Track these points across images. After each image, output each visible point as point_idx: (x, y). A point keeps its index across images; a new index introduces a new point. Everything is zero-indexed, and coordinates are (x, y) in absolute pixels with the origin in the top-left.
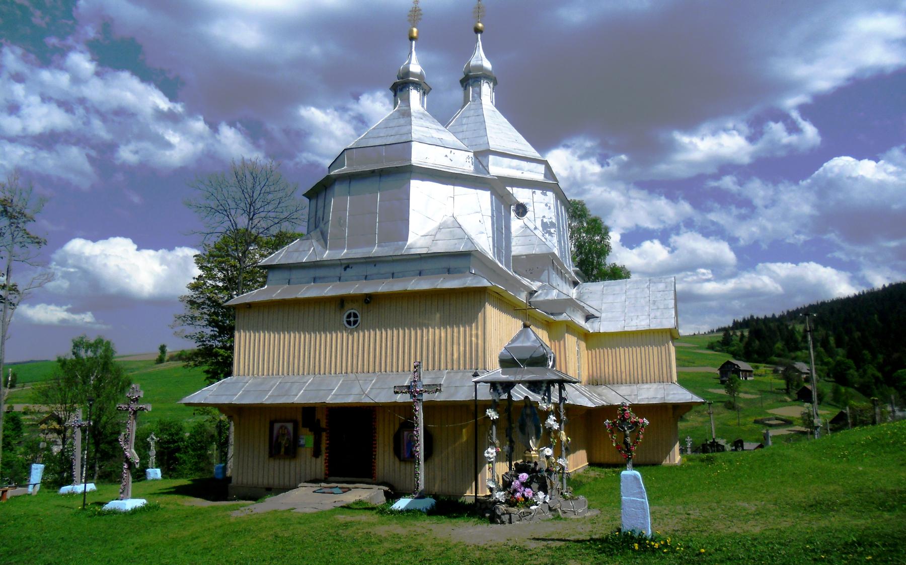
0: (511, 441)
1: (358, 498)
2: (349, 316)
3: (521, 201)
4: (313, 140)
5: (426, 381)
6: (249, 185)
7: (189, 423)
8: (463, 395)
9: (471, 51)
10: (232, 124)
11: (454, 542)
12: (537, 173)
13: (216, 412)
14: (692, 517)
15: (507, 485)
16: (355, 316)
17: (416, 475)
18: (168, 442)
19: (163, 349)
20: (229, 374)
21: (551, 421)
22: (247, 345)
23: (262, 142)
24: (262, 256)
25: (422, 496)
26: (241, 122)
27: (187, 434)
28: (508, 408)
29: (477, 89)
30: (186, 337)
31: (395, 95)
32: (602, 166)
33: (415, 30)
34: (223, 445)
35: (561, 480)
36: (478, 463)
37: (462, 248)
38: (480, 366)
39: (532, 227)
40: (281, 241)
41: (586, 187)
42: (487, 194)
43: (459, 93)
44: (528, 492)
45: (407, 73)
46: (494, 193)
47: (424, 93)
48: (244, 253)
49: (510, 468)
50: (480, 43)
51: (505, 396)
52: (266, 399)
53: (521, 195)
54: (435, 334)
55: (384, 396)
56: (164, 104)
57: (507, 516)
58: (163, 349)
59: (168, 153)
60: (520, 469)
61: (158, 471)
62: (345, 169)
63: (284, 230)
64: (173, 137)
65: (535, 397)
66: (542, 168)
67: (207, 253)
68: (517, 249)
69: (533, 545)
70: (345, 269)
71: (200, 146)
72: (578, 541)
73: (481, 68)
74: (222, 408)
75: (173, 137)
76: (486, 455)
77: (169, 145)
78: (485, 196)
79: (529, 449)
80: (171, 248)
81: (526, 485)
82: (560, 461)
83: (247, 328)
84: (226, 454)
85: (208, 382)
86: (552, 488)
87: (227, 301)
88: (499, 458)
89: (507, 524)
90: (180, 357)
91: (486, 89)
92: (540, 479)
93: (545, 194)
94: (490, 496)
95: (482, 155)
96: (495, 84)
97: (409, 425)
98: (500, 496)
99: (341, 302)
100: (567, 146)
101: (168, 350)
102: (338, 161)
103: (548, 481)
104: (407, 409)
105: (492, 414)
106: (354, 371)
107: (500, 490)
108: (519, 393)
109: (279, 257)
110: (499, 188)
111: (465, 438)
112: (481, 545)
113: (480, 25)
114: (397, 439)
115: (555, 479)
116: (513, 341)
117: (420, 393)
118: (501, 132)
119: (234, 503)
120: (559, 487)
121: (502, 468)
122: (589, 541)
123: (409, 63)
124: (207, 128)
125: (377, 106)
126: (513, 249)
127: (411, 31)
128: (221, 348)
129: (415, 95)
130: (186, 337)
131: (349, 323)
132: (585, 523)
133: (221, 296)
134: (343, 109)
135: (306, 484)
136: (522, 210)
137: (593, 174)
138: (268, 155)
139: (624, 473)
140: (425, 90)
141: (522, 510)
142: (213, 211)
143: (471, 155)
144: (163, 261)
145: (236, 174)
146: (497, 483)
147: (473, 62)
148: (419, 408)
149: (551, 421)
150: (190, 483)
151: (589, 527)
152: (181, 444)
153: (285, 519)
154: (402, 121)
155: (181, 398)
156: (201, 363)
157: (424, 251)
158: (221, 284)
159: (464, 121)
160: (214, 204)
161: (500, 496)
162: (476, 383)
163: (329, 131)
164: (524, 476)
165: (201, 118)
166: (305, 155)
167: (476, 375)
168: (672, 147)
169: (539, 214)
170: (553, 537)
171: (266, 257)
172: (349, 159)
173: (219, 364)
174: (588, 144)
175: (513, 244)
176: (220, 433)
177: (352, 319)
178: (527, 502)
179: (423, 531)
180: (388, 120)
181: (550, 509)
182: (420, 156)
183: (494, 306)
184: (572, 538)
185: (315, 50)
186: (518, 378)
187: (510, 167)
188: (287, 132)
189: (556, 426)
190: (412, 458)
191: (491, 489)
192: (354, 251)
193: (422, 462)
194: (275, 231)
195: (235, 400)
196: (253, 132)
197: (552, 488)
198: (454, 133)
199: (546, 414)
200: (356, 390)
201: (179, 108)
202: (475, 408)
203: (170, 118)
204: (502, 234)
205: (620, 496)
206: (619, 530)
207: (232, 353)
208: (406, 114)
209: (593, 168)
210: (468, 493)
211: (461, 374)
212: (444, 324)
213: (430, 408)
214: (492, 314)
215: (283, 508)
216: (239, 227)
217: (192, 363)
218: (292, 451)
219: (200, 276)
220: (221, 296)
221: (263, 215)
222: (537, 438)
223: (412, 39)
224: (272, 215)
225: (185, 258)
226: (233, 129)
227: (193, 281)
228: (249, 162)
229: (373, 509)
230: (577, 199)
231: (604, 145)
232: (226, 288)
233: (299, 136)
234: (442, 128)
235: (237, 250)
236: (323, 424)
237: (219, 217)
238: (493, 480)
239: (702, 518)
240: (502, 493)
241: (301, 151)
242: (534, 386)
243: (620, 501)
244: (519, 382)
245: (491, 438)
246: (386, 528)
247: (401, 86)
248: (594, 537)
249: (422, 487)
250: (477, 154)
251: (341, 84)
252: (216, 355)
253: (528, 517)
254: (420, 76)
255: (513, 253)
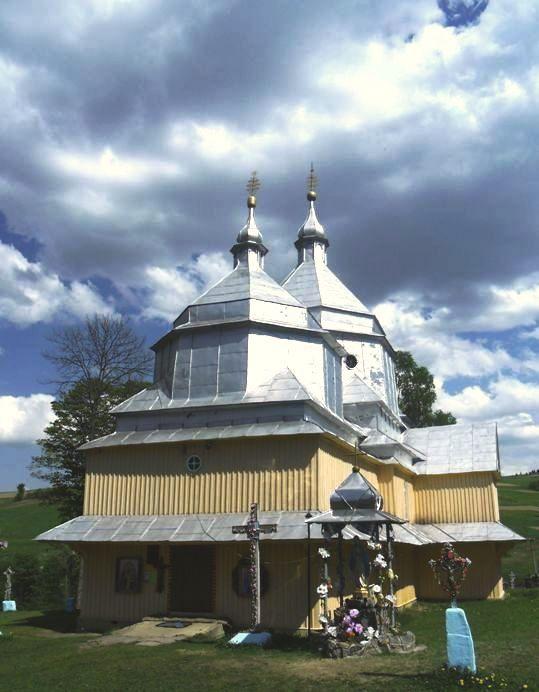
0: (342, 578)
1: (198, 632)
2: (191, 461)
3: (351, 352)
4: (158, 297)
5: (263, 520)
6: (96, 339)
7: (43, 557)
8: (298, 534)
9: (305, 216)
10: (84, 282)
11: (289, 675)
12: (365, 327)
13: (67, 546)
14: (515, 652)
15: (338, 621)
16: (197, 460)
17: (254, 610)
18: (24, 575)
19: (21, 487)
20: (81, 513)
21: (380, 559)
22: (96, 486)
23: (111, 299)
24: (113, 403)
25: (258, 630)
26: (91, 280)
27: (42, 567)
28: (339, 547)
29: (311, 251)
30: (43, 477)
31: (235, 257)
32: (426, 319)
33: (253, 198)
34: (74, 580)
35: (390, 616)
36: (312, 599)
37: (296, 397)
38: (314, 507)
39: (362, 377)
40: (131, 389)
41: (412, 338)
42: (320, 346)
43: (294, 253)
44: (359, 627)
45: (246, 237)
46: (326, 345)
47: (262, 255)
48: (96, 400)
49: (341, 604)
50: (313, 210)
51: (336, 536)
52: (113, 537)
53: (350, 347)
54: (271, 477)
55: (225, 536)
56: (22, 264)
57: (339, 651)
58: (21, 487)
59: (27, 308)
60: (351, 605)
61: (13, 603)
62: (189, 324)
63: (132, 379)
64: (32, 294)
65: (362, 536)
66: (370, 322)
67: (63, 400)
68: (349, 397)
69: (363, 680)
70: (188, 416)
71: (57, 302)
72: (406, 676)
73: (314, 232)
74: (73, 544)
75: (32, 294)
76: (319, 591)
77: (28, 302)
78: (316, 350)
79: (359, 586)
80: (27, 395)
81: (356, 620)
82: (388, 597)
83: (97, 471)
84: (77, 586)
85: (61, 519)
86: (381, 624)
87: (79, 445)
88: (331, 594)
89: (339, 659)
90: (38, 494)
91: (319, 251)
92: (369, 616)
93: (373, 347)
94: (323, 631)
95: (314, 310)
96: (327, 246)
97: (247, 562)
98: (332, 630)
99: (184, 446)
100: (393, 301)
101: (26, 488)
102: (183, 318)
103: (377, 617)
104: (244, 547)
105: (324, 553)
106: (196, 511)
107: (332, 625)
108: (349, 533)
109: (128, 405)
110: (329, 341)
111: (299, 575)
112: (314, 678)
113: (313, 193)
114: (235, 574)
115: (383, 614)
116: (343, 484)
117: (257, 533)
118: (333, 290)
119: (82, 635)
120: (388, 622)
121: (334, 604)
122: (416, 676)
123: (248, 227)
124: (62, 285)
125: (217, 267)
126: (344, 397)
127: (249, 200)
128: (74, 488)
129: (252, 256)
130: (43, 477)
131: (191, 467)
132: (412, 659)
133: (74, 439)
134: (182, 269)
135: (149, 618)
136: (352, 361)
137: (416, 326)
138: (117, 310)
139: (448, 610)
140: (262, 251)
141: (353, 645)
142: (67, 362)
143: (305, 311)
144: (21, 407)
145: (90, 327)
146: (329, 619)
147: (307, 226)
148: (256, 547)
149: (380, 559)
150: (41, 614)
151: (417, 663)
152: (36, 577)
153: (131, 650)
154: (241, 280)
155: (35, 537)
156: (55, 502)
157: (261, 400)
158: (75, 429)
159: (299, 279)
160: (68, 355)
161: (332, 630)
162: (309, 523)
163: (171, 291)
164: (355, 612)
165: (56, 276)
166: (149, 310)
167: (309, 516)
168: (489, 300)
169: (368, 366)
170: (383, 672)
171: (117, 404)
172: (193, 315)
173: (71, 504)
174: (411, 299)
175: (344, 392)
176: (71, 567)
177: (194, 463)
178: (359, 637)
179: (259, 665)
180: (228, 279)
181: (379, 644)
182: (258, 313)
183: (326, 451)
184: (401, 673)
185: (161, 217)
186: (348, 519)
187: (341, 322)
188: (133, 290)
189: (384, 565)
190: (249, 594)
191: (324, 624)
192: (196, 400)
193: (258, 599)
194: (125, 380)
195: (85, 538)
196: (104, 289)
197: (381, 624)
198: (289, 291)
199: (375, 553)
200: (198, 530)
201: (37, 268)
202: (307, 546)
203: (30, 277)
204: (333, 385)
205: (446, 633)
206: (445, 666)
207: (83, 493)
208: (245, 274)
209: (416, 320)
210: (302, 627)
211: (295, 515)
212: (279, 468)
213: (266, 545)
214: (324, 458)
215: (128, 641)
216: (92, 376)
217: (47, 501)
218: (137, 586)
219: (56, 422)
220: (74, 439)
221: (114, 365)
222: (366, 575)
223: (250, 205)
224: (122, 365)
225: (42, 404)
226: (85, 286)
227: (50, 426)
228: (101, 318)
229: (212, 643)
230: (403, 350)
231: (426, 299)
232: (78, 433)
233: (145, 293)
234: (277, 286)
235: (89, 398)
236: (167, 562)
237: (73, 367)
238: (325, 615)
239: (524, 654)
240: (334, 628)
241: (147, 306)
242: (362, 526)
243: (446, 638)
244: (349, 523)
245: (323, 576)
246: (223, 662)
247: (241, 248)
248: (422, 672)
249: (258, 621)
250: (310, 310)
251: (184, 247)
252: (70, 494)
253: (359, 651)
254: (258, 240)
255: (344, 402)
